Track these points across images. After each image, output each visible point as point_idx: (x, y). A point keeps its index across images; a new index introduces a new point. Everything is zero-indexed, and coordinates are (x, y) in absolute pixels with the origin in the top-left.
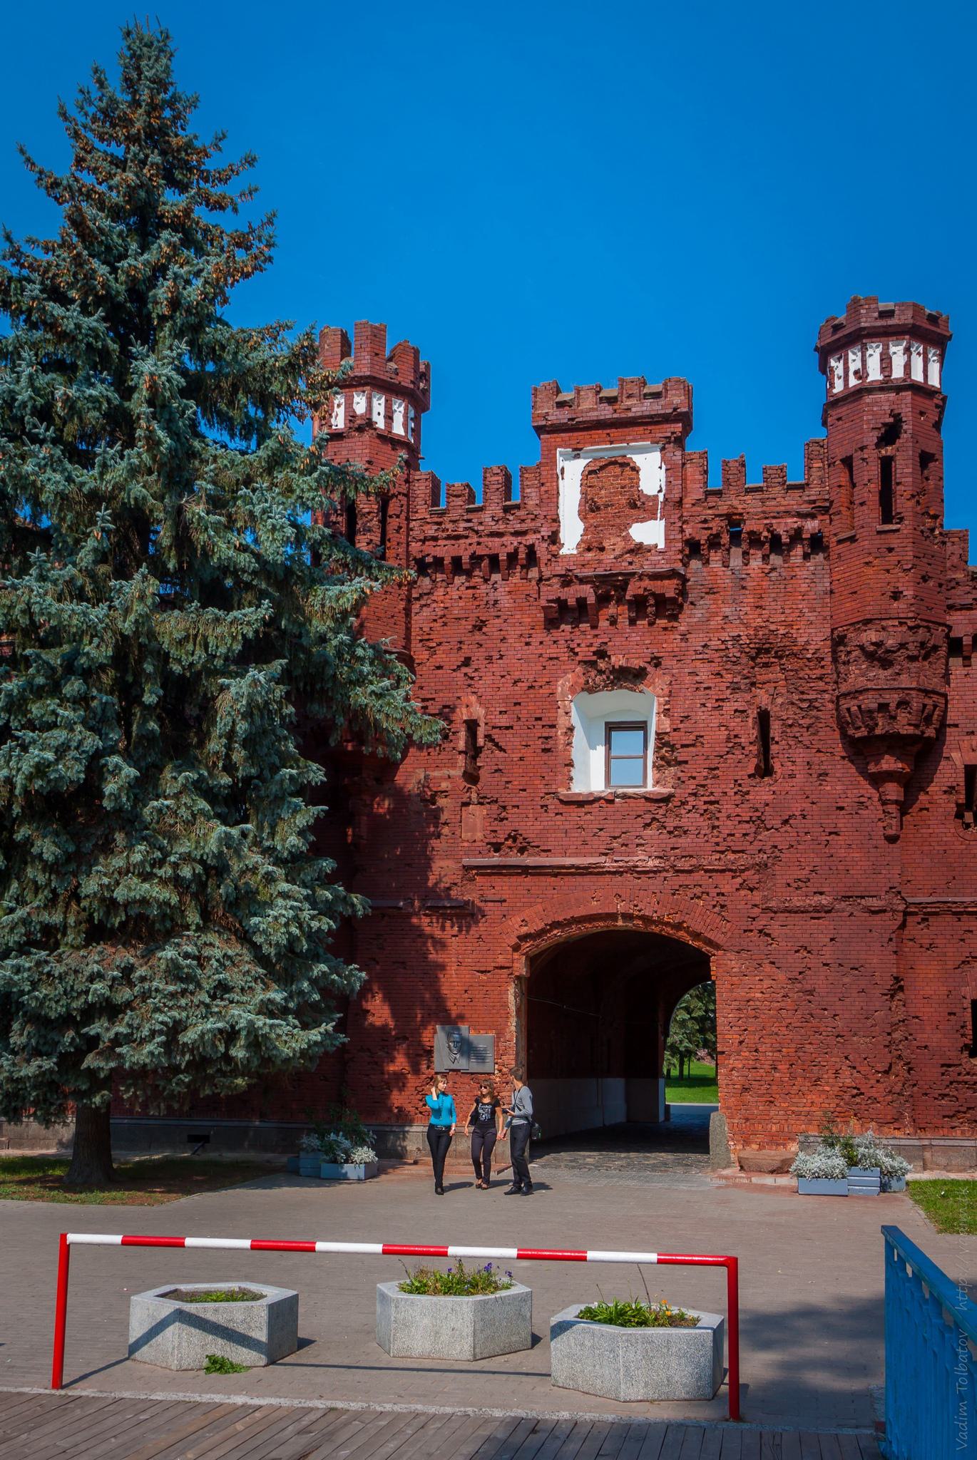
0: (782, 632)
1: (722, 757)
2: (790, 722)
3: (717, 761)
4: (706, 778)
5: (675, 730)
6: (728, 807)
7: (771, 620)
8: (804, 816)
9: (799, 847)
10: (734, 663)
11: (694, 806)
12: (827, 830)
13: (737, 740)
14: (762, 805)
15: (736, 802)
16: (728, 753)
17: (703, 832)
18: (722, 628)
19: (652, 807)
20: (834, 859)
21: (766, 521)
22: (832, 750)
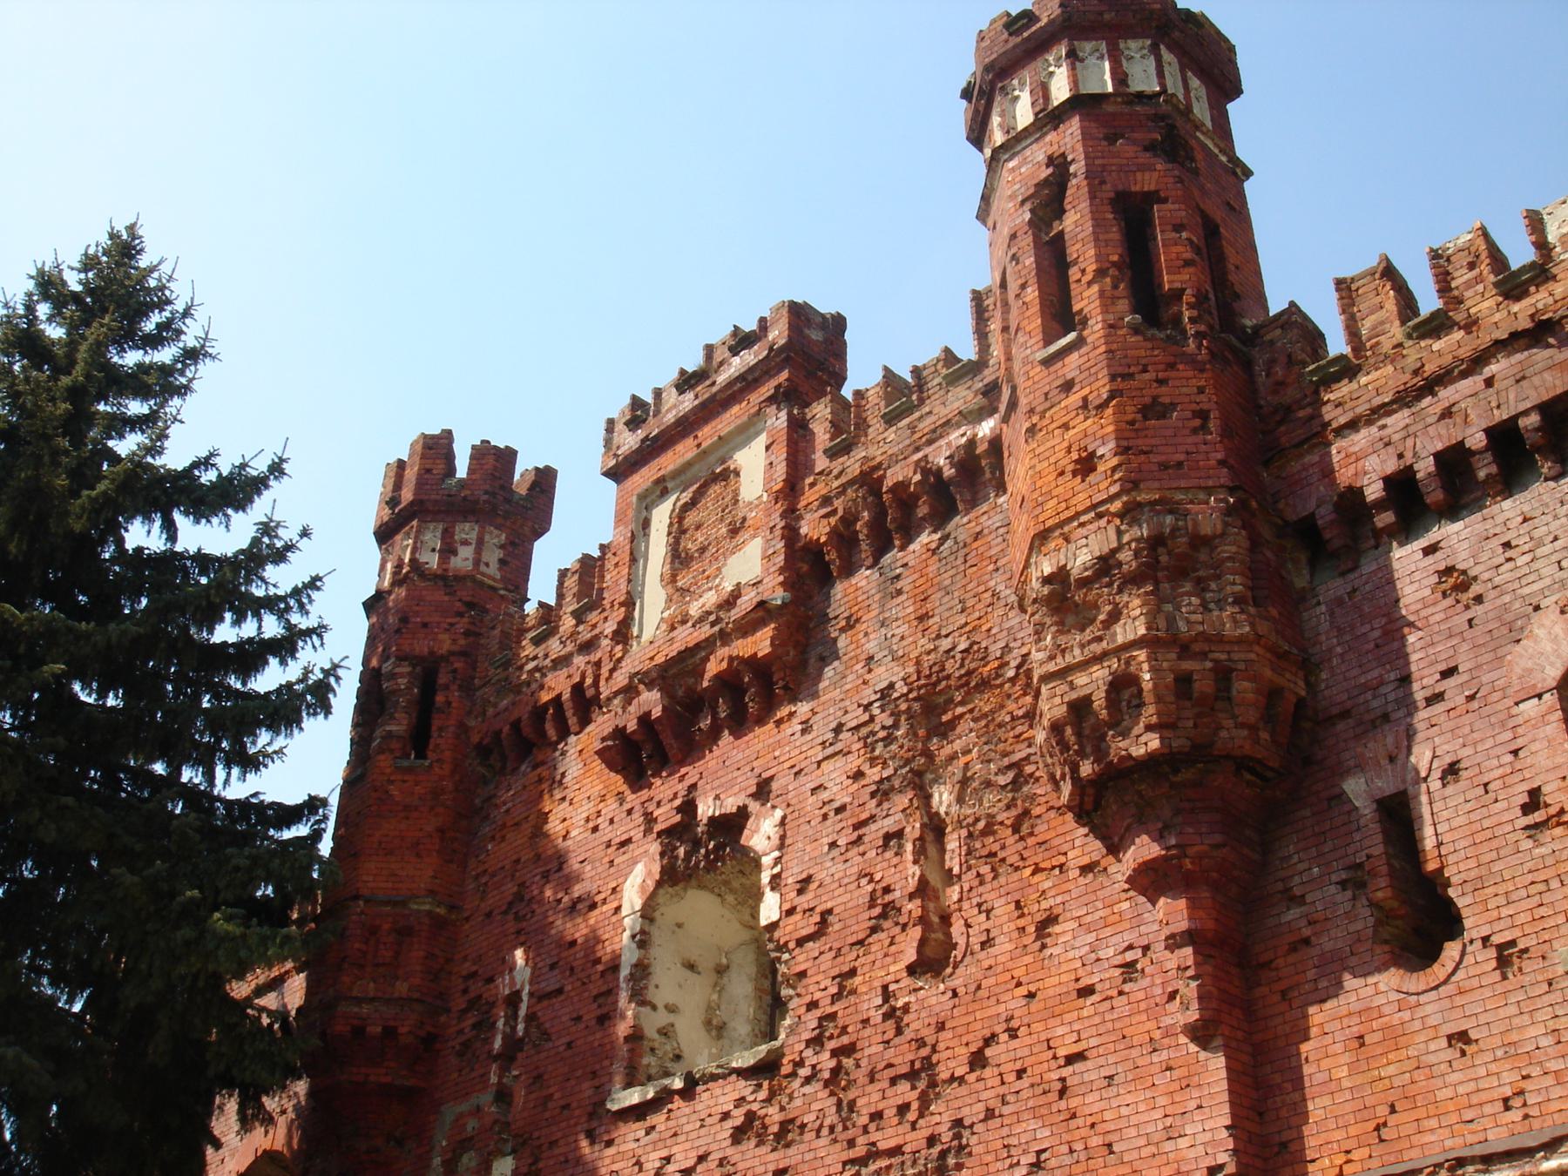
0: (962, 647)
1: (861, 943)
2: (981, 825)
3: (854, 955)
4: (835, 998)
5: (791, 912)
6: (871, 1050)
7: (944, 632)
8: (1013, 1034)
9: (1006, 1110)
10: (889, 740)
11: (814, 1067)
12: (1062, 1052)
13: (888, 898)
14: (932, 1029)
15: (886, 1037)
16: (874, 930)
17: (827, 1122)
18: (865, 683)
19: (743, 1087)
20: (1079, 1121)
21: (919, 455)
22: (1062, 859)
